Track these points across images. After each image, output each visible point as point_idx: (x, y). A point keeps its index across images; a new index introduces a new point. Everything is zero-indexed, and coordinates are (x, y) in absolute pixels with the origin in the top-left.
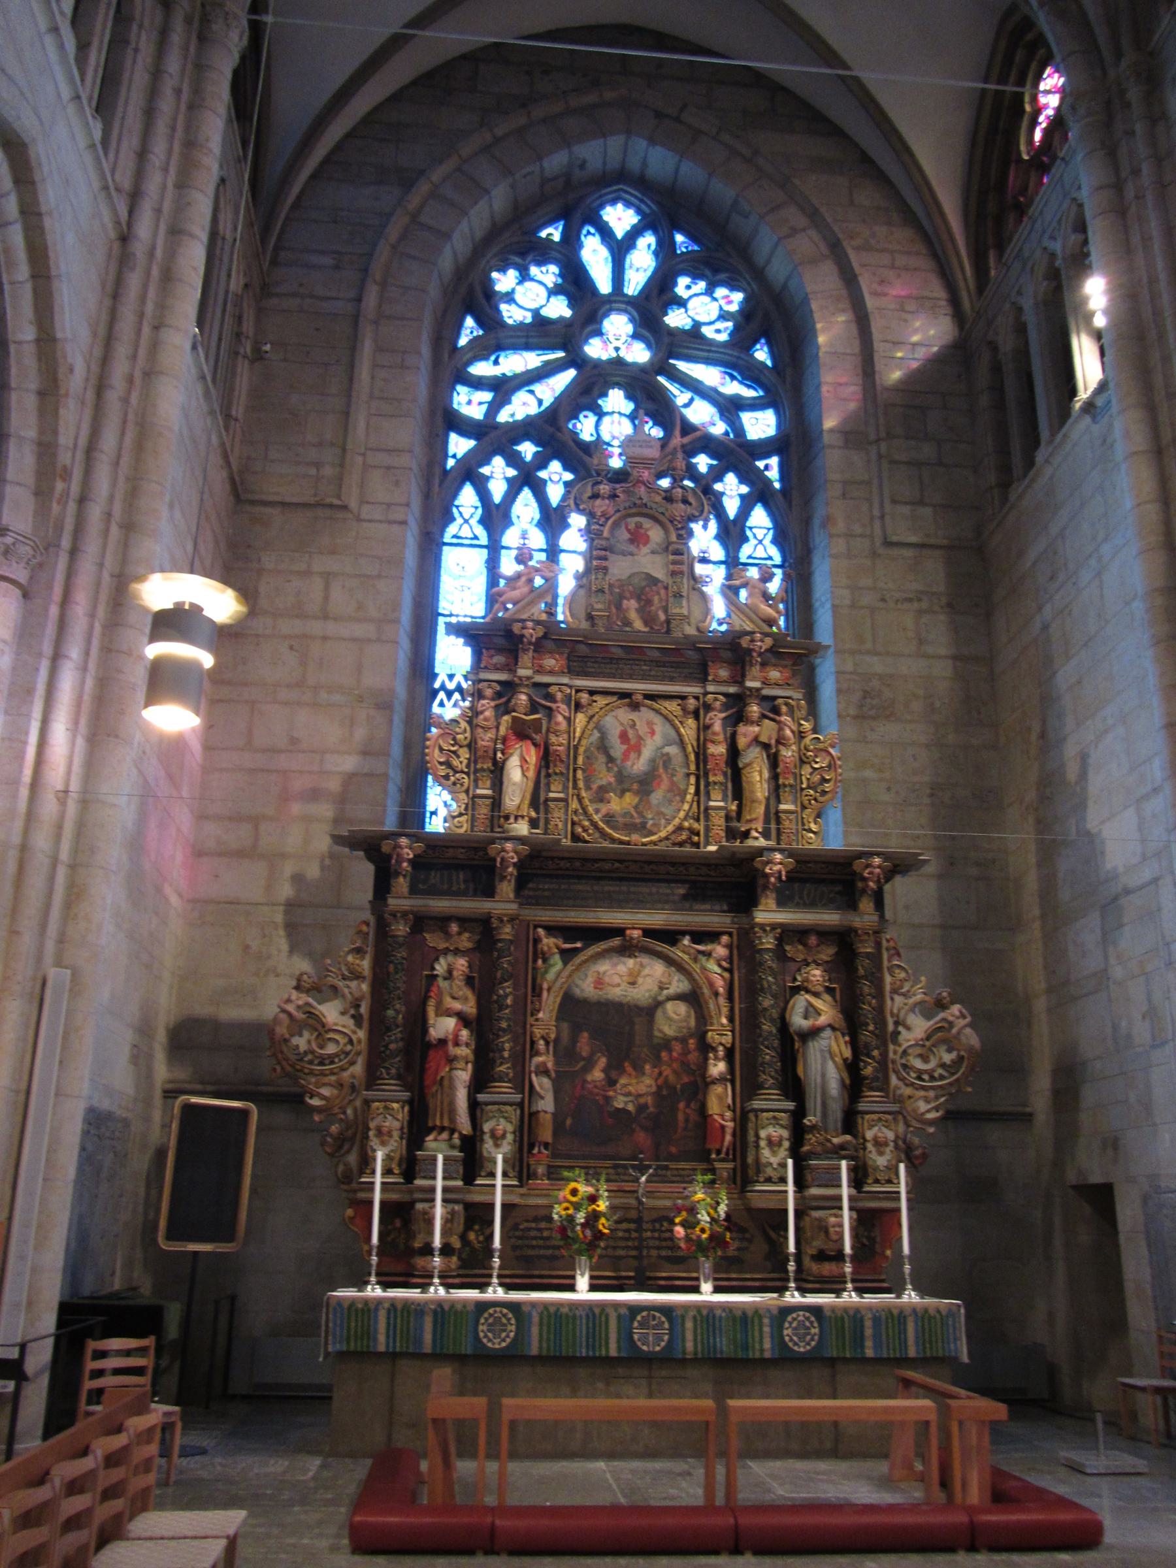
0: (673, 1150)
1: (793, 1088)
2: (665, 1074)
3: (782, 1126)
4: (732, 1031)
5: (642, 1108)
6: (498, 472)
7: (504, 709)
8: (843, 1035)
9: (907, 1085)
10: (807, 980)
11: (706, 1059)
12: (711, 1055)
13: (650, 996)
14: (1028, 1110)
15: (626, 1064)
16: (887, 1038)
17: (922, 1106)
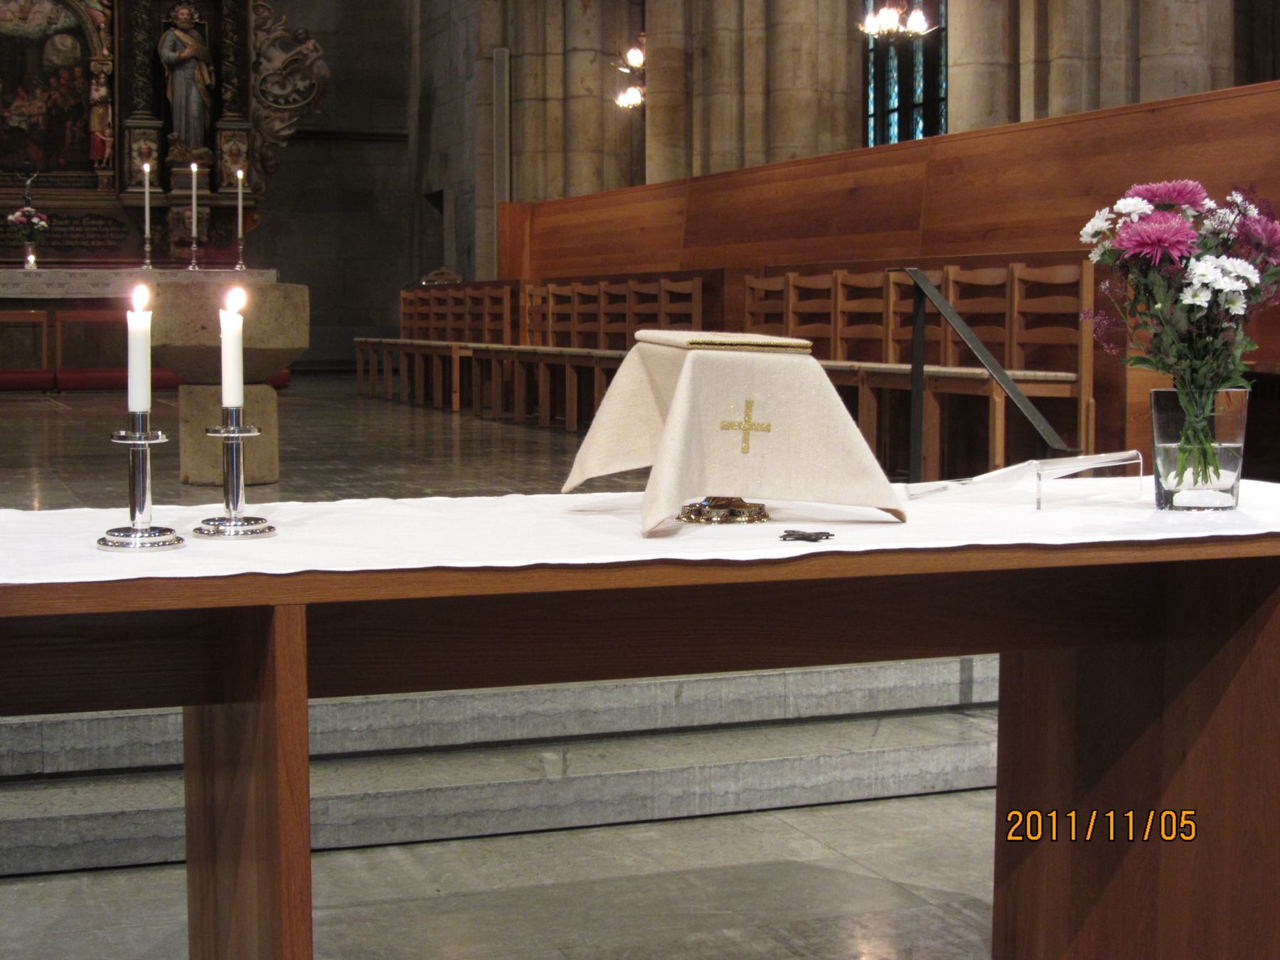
0: (62, 161)
1: (162, 109)
2: (54, 96)
3: (151, 140)
4: (113, 61)
5: (33, 126)
8: (208, 65)
9: (264, 107)
10: (177, 18)
11: (90, 84)
12: (94, 81)
13: (40, 30)
14: (405, 132)
15: (20, 89)
16: (245, 66)
17: (278, 125)
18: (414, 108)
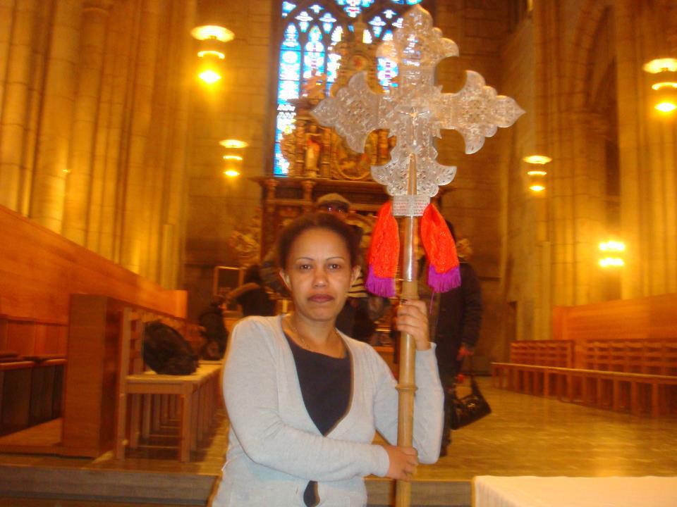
6: (304, 18)
7: (307, 131)
18: (503, 267)
